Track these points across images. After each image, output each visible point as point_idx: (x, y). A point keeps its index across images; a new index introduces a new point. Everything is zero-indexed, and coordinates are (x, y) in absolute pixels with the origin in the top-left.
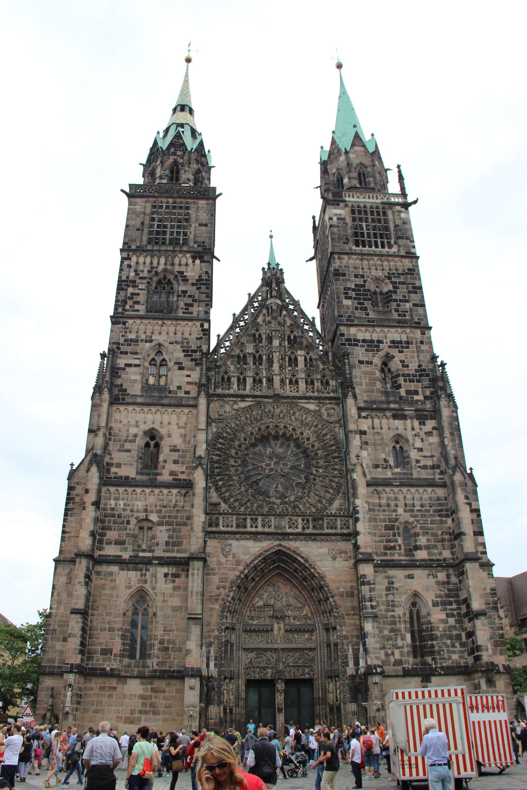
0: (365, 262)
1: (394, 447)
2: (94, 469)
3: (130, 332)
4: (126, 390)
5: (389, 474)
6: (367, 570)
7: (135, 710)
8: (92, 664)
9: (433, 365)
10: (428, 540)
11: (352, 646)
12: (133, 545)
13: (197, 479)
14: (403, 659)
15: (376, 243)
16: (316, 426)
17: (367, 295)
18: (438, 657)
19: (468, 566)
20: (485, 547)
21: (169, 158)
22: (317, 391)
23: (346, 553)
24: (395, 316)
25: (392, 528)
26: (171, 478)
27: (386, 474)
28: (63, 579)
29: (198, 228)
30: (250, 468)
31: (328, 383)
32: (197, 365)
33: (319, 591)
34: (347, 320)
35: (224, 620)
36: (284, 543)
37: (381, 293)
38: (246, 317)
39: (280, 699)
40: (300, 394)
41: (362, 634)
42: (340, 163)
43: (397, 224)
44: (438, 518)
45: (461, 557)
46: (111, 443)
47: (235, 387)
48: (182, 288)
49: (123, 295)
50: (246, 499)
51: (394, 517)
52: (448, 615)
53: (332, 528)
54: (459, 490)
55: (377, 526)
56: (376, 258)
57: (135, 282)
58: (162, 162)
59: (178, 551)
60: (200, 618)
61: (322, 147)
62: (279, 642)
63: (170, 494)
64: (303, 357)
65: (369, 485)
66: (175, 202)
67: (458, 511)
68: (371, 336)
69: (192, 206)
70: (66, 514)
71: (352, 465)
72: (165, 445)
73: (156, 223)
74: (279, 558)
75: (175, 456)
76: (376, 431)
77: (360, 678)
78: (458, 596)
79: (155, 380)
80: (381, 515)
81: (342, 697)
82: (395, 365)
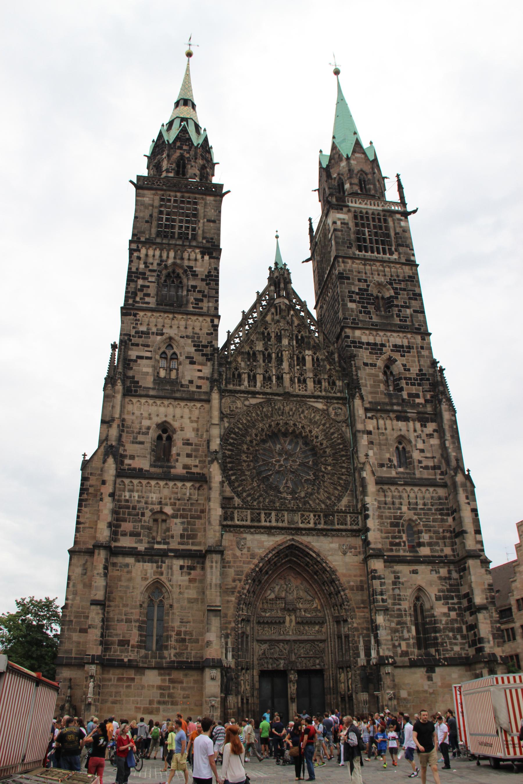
0: (368, 267)
1: (397, 448)
2: (111, 460)
3: (141, 324)
4: (138, 382)
5: (393, 473)
6: (377, 565)
7: (153, 701)
8: (109, 655)
9: (433, 370)
10: (431, 537)
11: (363, 637)
12: (148, 536)
13: (213, 473)
14: (409, 650)
15: (378, 249)
16: (324, 425)
17: (370, 299)
18: (441, 648)
19: (471, 563)
20: (482, 545)
21: (175, 152)
22: (325, 390)
23: (355, 548)
24: (397, 321)
25: (397, 525)
26: (185, 471)
27: (391, 473)
28: (79, 570)
29: (206, 224)
30: (261, 463)
31: (334, 383)
32: (208, 360)
33: (330, 585)
34: (352, 323)
35: (241, 612)
36: (297, 538)
37: (383, 298)
38: (255, 315)
39: (292, 688)
40: (308, 393)
41: (372, 626)
42: (341, 168)
43: (397, 231)
44: (439, 517)
45: (462, 554)
46: (124, 435)
47: (246, 383)
48: (192, 283)
49: (134, 286)
50: (258, 494)
51: (398, 514)
52: (450, 609)
53: (342, 524)
54: (461, 491)
55: (383, 523)
56: (378, 264)
57: (144, 274)
58: (168, 156)
59: (193, 544)
60: (220, 610)
61: (321, 151)
62: (291, 633)
63: (184, 487)
64: (311, 357)
65: (377, 483)
66: (183, 197)
67: (459, 510)
68: (375, 339)
69: (200, 201)
70: (80, 505)
71: (360, 463)
72: (178, 438)
73: (164, 217)
74: (291, 552)
75: (188, 449)
76: (380, 431)
77: (371, 668)
78: (459, 592)
79: (166, 373)
80: (387, 513)
81: (354, 686)
82: (397, 368)
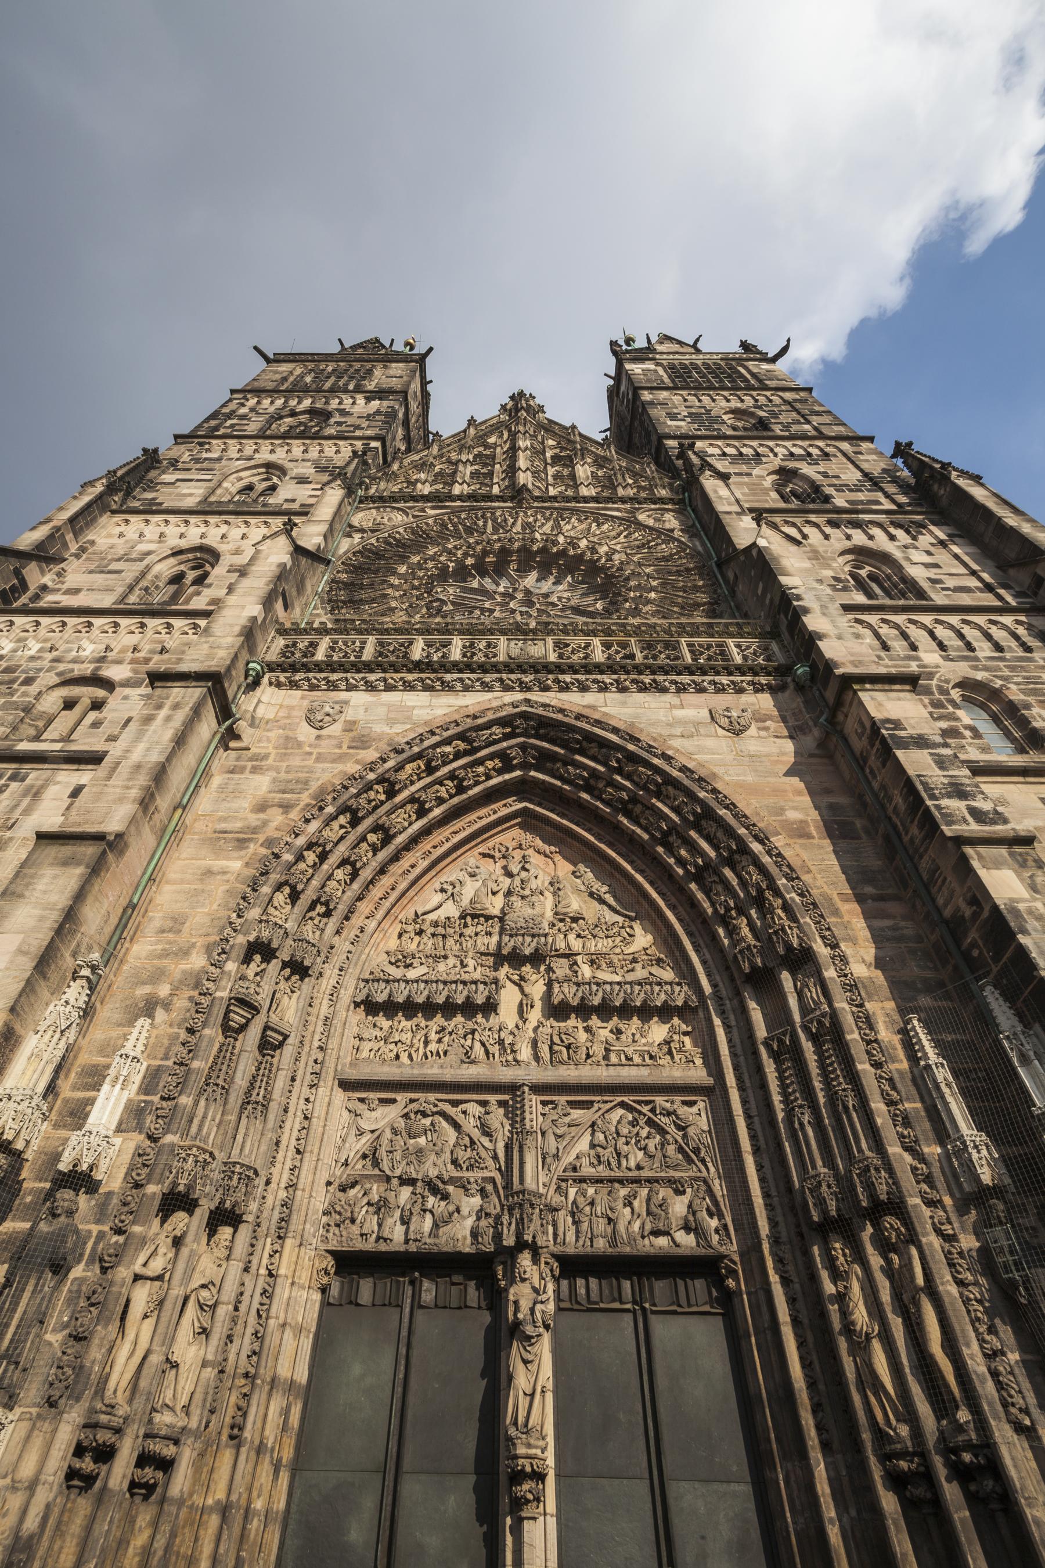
35: (254, 913)
74: (523, 747)
